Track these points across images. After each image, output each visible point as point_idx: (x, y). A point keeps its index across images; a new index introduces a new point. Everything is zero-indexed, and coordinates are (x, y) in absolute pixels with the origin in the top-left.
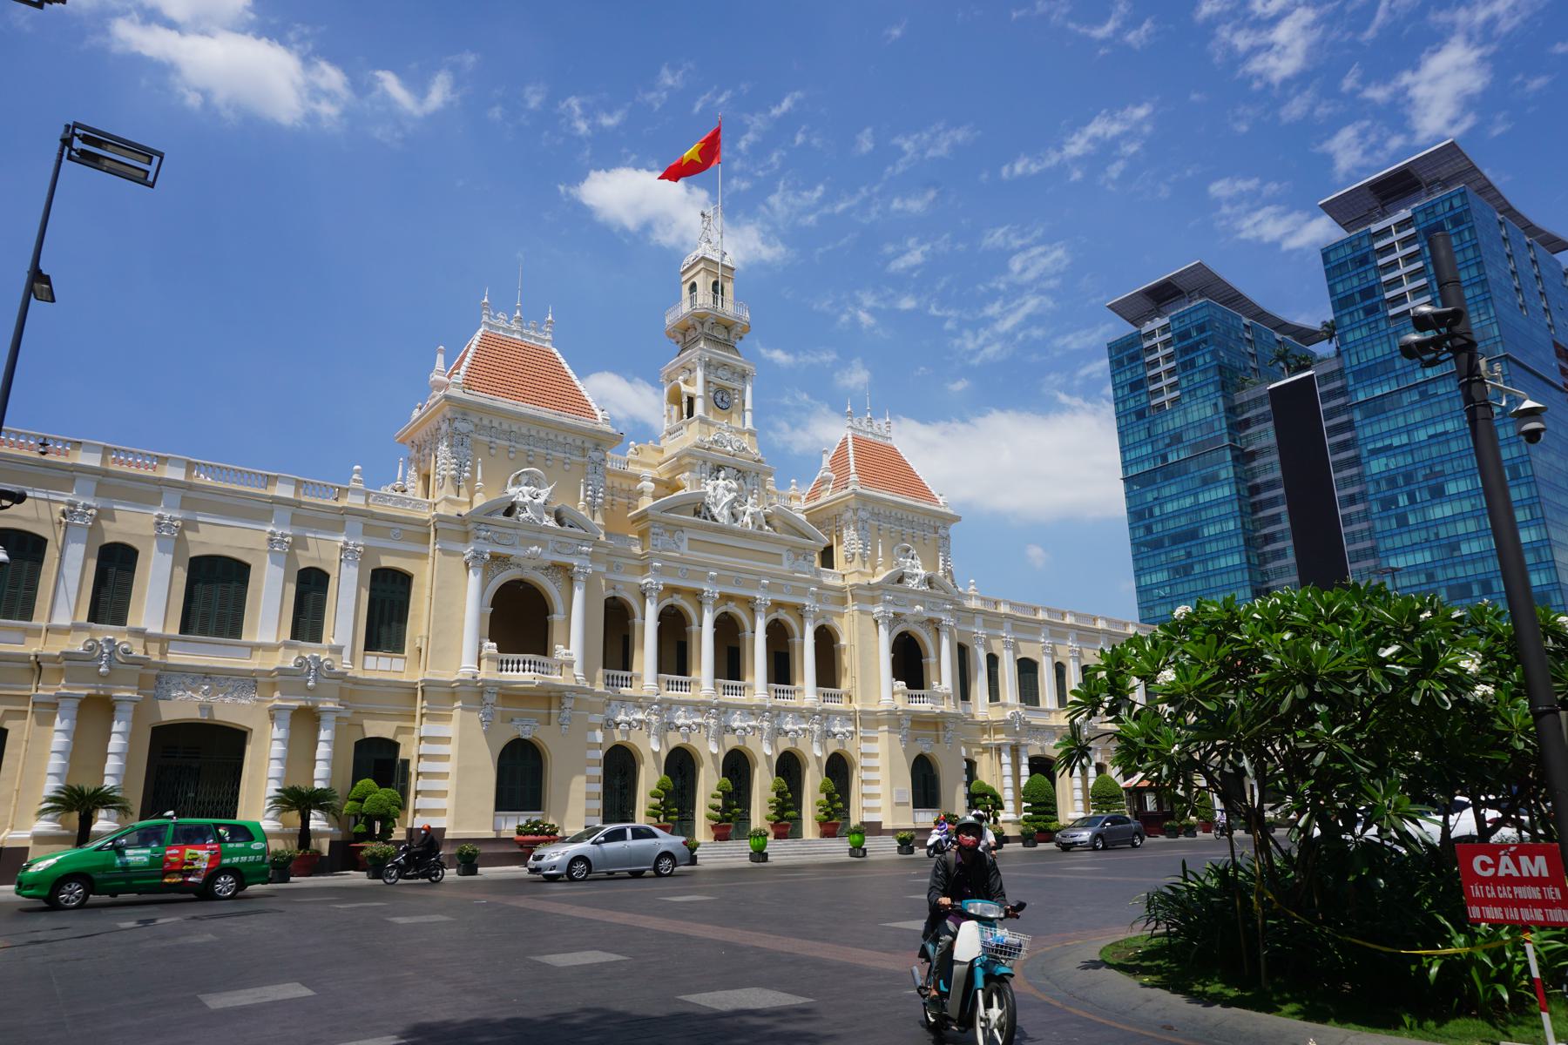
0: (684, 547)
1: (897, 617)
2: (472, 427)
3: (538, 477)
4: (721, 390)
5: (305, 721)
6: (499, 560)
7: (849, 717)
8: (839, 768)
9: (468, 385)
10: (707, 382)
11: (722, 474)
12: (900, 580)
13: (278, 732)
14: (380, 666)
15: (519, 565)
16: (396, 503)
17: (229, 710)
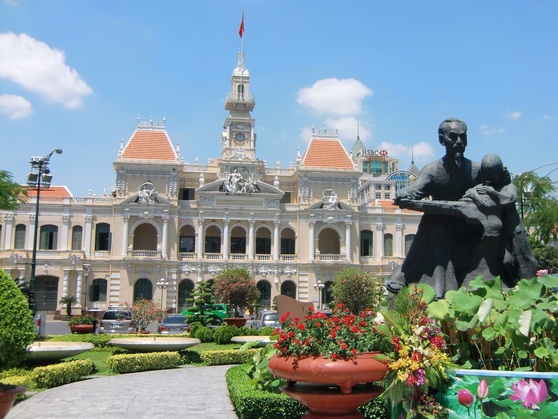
0: (215, 203)
1: (319, 223)
5: (72, 275)
7: (295, 266)
9: (125, 156)
10: (231, 132)
11: (235, 171)
12: (322, 206)
13: (66, 278)
14: (101, 256)
15: (143, 219)
16: (103, 201)
17: (53, 271)
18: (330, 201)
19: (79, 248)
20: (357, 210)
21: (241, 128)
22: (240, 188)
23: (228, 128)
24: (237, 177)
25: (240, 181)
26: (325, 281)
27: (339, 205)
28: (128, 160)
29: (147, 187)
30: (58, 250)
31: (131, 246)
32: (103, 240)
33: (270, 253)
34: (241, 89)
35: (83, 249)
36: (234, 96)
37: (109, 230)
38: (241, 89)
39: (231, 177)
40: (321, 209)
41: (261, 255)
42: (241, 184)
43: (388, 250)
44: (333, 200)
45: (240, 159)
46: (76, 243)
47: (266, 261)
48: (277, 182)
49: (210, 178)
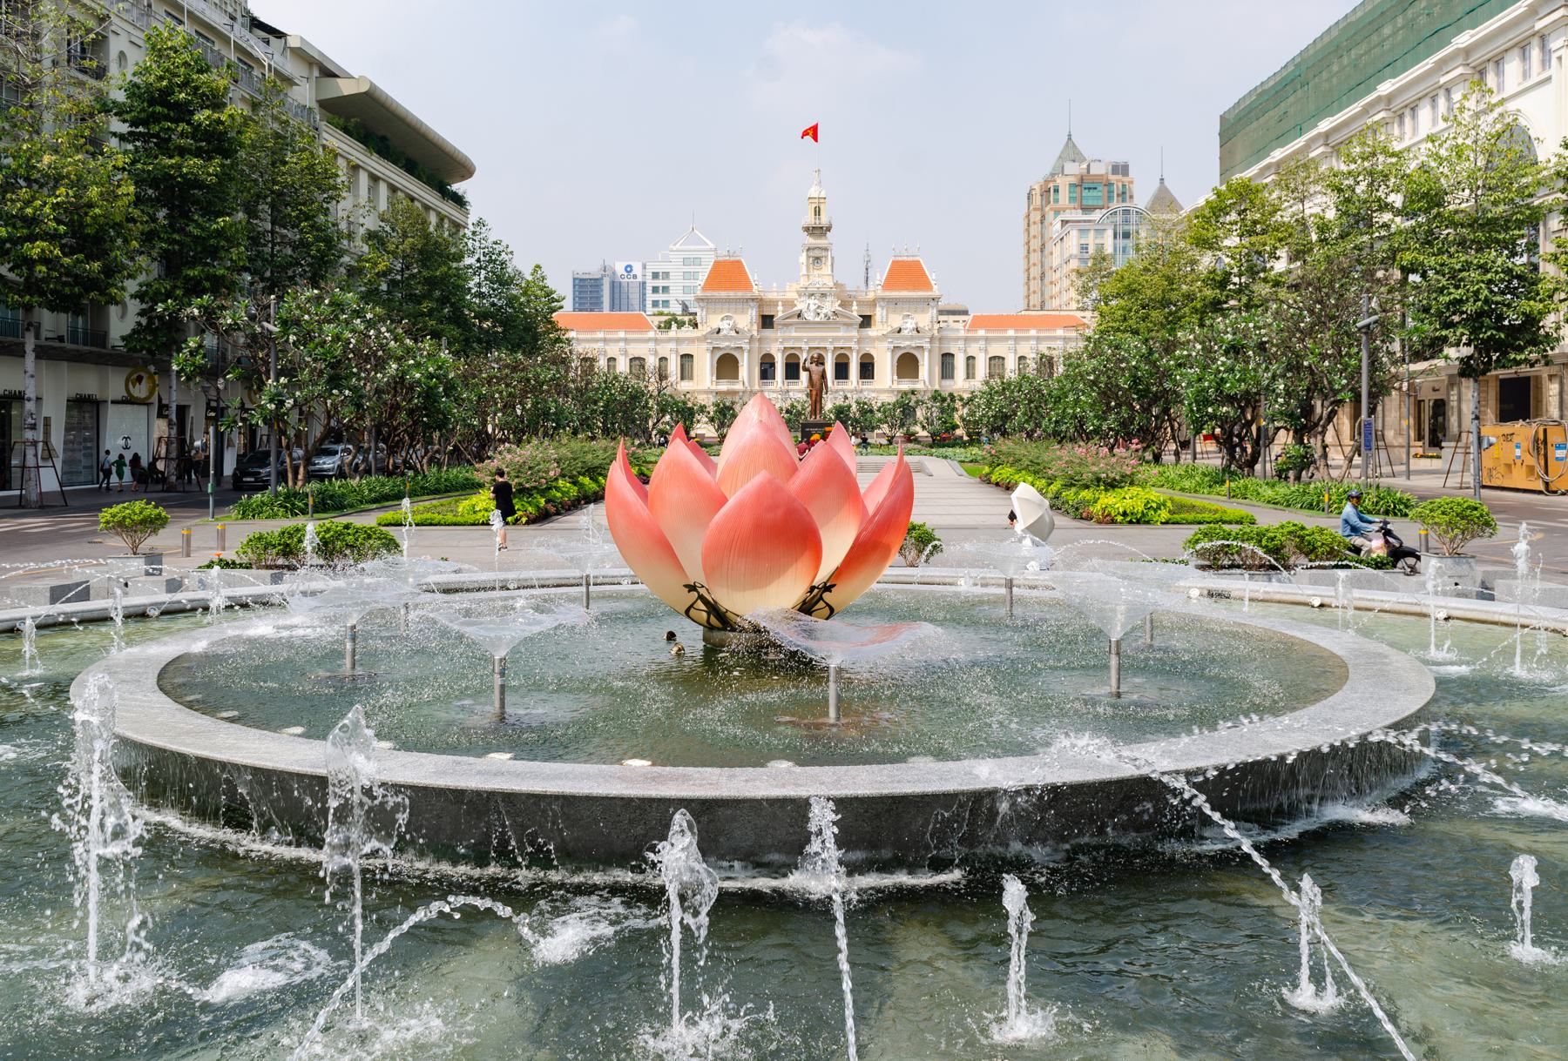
4: (817, 258)
9: (704, 288)
21: (817, 253)
28: (709, 294)
29: (728, 317)
36: (810, 219)
43: (970, 374)
44: (910, 324)
49: (789, 304)
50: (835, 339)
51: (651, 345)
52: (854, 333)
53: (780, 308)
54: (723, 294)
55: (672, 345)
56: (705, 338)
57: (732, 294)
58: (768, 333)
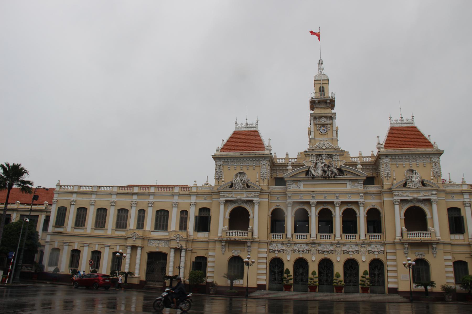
2: (222, 163)
3: (244, 173)
6: (228, 202)
8: (377, 266)
10: (315, 125)
11: (320, 158)
12: (405, 185)
14: (202, 235)
18: (414, 179)
19: (185, 229)
20: (441, 187)
21: (323, 121)
22: (325, 172)
23: (312, 122)
24: (322, 163)
25: (325, 165)
26: (416, 258)
27: (423, 184)
30: (168, 230)
31: (227, 227)
32: (203, 223)
33: (357, 233)
34: (322, 90)
35: (188, 230)
37: (209, 214)
38: (322, 90)
39: (316, 164)
40: (404, 189)
41: (347, 234)
42: (326, 169)
44: (416, 179)
45: (324, 147)
46: (183, 225)
47: (353, 241)
48: (359, 166)
50: (342, 193)
51: (176, 199)
52: (359, 187)
53: (290, 167)
54: (238, 153)
55: (193, 199)
56: (218, 192)
57: (246, 153)
58: (278, 189)
